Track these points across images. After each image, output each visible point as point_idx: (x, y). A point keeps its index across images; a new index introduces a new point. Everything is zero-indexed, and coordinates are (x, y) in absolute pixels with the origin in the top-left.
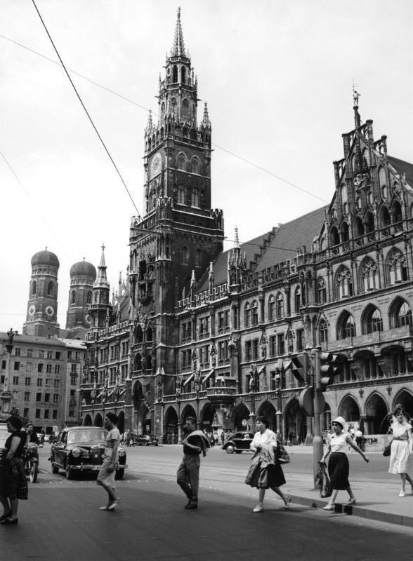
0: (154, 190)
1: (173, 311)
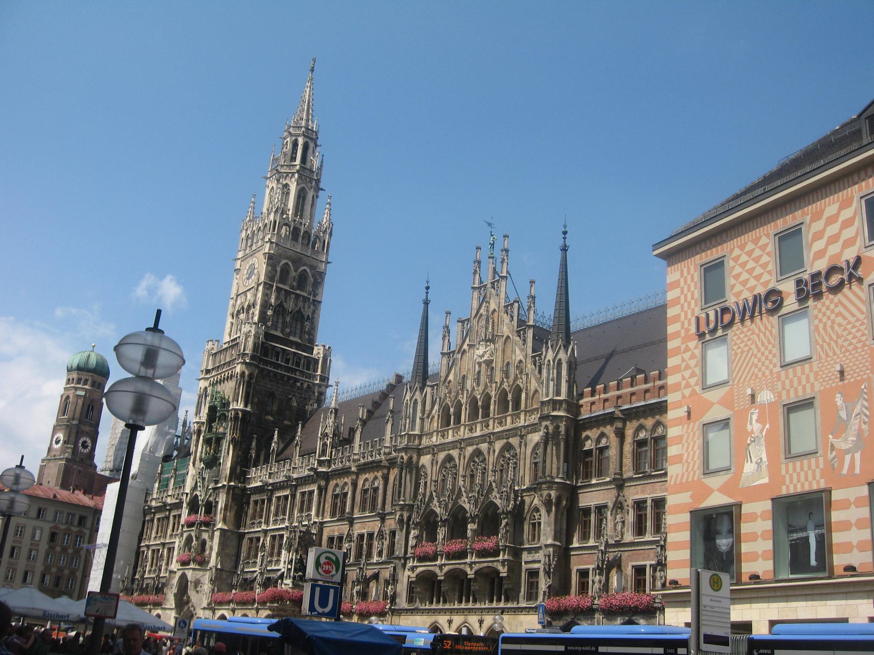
0: (243, 308)
1: (244, 482)
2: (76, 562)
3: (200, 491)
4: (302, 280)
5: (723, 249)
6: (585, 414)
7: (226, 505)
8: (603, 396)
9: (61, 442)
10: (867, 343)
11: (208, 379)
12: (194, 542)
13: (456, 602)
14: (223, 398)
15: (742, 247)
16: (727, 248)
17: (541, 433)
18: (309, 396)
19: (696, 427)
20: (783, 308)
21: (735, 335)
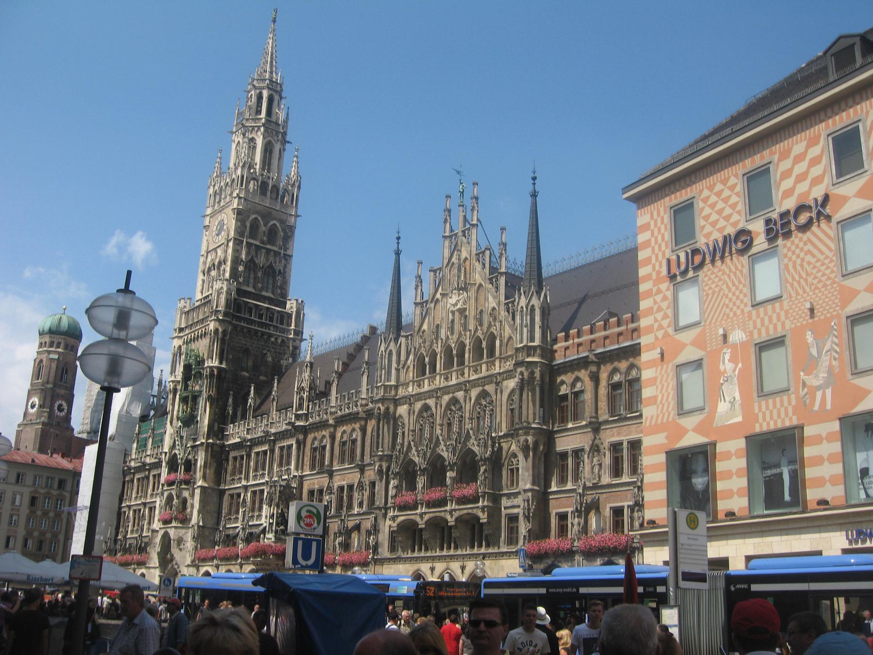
0: (214, 265)
2: (58, 525)
3: (179, 450)
4: (272, 234)
5: (692, 191)
6: (559, 360)
7: (205, 463)
8: (576, 340)
9: (37, 406)
10: (837, 280)
11: (181, 337)
12: (175, 501)
13: (438, 550)
14: (197, 356)
15: (711, 188)
16: (696, 189)
17: (516, 380)
18: (284, 350)
19: (669, 371)
20: (753, 248)
21: (706, 276)
